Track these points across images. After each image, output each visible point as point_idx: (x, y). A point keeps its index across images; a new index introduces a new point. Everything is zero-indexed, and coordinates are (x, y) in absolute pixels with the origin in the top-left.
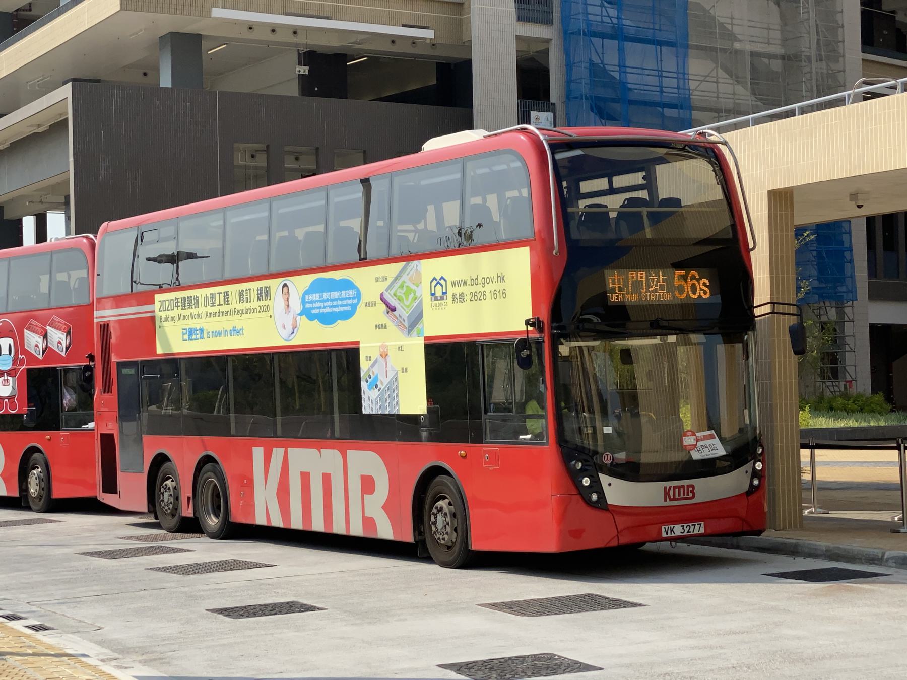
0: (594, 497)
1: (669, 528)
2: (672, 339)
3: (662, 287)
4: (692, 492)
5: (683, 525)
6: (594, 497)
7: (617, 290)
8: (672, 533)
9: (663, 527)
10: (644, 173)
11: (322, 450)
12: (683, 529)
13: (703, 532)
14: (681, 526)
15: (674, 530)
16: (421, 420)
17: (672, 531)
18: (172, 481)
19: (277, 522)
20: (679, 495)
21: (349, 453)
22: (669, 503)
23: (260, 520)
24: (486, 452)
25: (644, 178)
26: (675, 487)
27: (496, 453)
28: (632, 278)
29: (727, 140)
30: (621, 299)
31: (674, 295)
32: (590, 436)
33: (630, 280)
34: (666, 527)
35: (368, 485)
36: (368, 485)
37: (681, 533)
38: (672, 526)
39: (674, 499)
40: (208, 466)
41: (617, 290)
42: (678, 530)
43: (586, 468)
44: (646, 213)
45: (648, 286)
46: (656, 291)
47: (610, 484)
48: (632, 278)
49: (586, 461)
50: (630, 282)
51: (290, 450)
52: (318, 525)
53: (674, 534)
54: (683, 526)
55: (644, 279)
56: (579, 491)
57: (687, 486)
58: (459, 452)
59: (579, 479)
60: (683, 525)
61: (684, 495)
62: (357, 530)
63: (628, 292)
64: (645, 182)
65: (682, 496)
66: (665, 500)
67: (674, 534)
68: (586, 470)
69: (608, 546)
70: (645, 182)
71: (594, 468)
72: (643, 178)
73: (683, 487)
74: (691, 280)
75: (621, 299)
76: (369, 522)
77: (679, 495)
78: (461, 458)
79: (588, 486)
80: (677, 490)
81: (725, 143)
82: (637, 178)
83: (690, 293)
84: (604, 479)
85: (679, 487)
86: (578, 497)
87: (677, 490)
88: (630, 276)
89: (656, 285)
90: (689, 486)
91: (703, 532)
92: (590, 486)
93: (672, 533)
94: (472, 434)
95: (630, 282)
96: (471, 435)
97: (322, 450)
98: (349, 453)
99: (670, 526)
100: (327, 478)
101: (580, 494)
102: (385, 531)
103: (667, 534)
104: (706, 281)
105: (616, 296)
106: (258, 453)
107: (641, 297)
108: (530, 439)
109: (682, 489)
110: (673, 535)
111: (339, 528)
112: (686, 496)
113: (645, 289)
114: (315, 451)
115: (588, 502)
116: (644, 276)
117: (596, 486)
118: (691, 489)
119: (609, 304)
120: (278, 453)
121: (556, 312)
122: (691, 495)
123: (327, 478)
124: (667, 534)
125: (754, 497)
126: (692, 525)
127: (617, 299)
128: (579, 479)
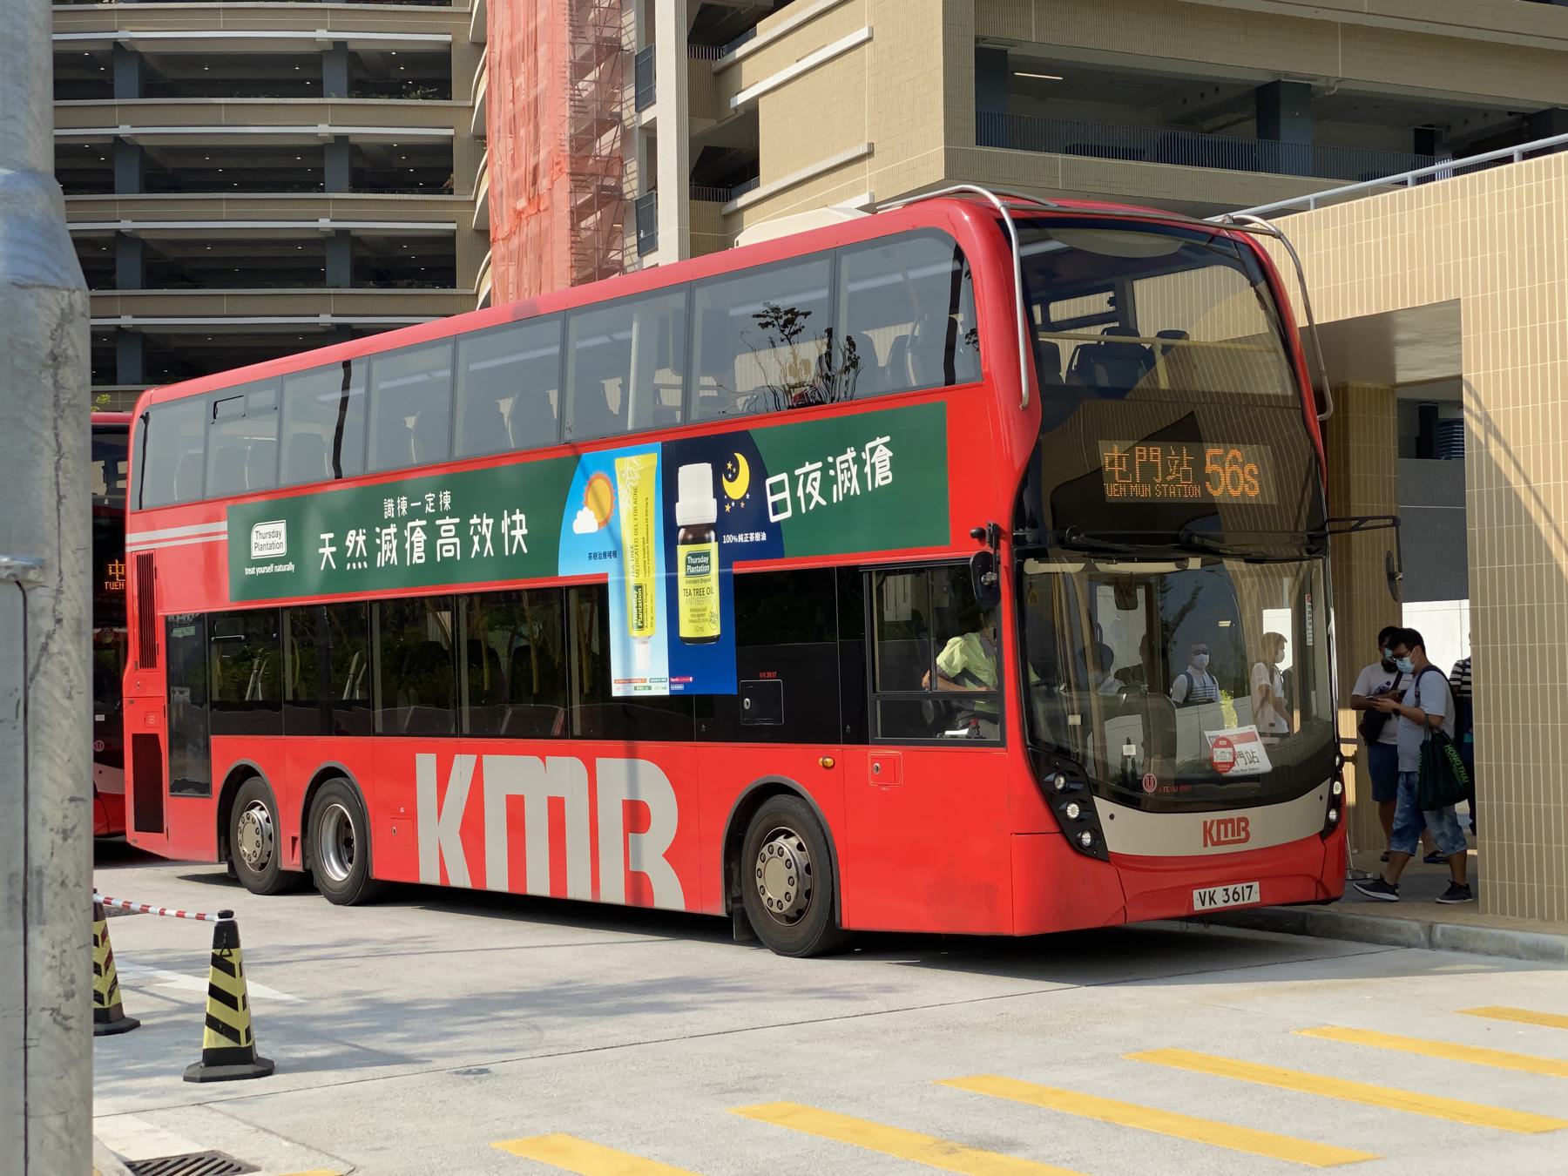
0: (1087, 838)
1: (1246, 897)
2: (1195, 563)
3: (1186, 475)
4: (1245, 829)
5: (1226, 887)
6: (1087, 838)
7: (1117, 478)
8: (1212, 902)
9: (1196, 893)
10: (1111, 294)
11: (547, 758)
12: (1227, 894)
13: (1258, 899)
14: (1224, 890)
15: (1214, 897)
16: (745, 706)
17: (1211, 899)
18: (262, 809)
19: (460, 878)
20: (1226, 836)
21: (600, 762)
22: (1212, 850)
23: (428, 875)
24: (876, 759)
25: (1111, 302)
26: (1220, 822)
27: (894, 760)
28: (1141, 457)
29: (1282, 231)
30: (1123, 492)
31: (1204, 489)
32: (1078, 731)
33: (1138, 460)
34: (1202, 891)
35: (636, 816)
36: (636, 816)
37: (1224, 901)
38: (1212, 890)
39: (1219, 843)
40: (330, 785)
41: (1117, 478)
42: (1220, 898)
43: (1073, 786)
44: (1160, 347)
45: (1166, 473)
46: (1176, 481)
47: (1112, 817)
48: (1141, 457)
49: (1072, 774)
50: (1137, 466)
51: (486, 758)
52: (538, 885)
53: (1215, 903)
54: (1226, 890)
55: (1159, 461)
56: (1061, 828)
57: (1238, 819)
58: (821, 760)
59: (1061, 808)
60: (1226, 887)
61: (1233, 835)
62: (614, 893)
63: (1134, 483)
64: (1112, 308)
65: (1230, 837)
66: (1206, 845)
67: (1215, 903)
68: (1072, 791)
69: (1110, 924)
70: (1112, 308)
71: (1085, 791)
72: (1108, 302)
73: (1231, 821)
74: (1231, 466)
75: (1123, 492)
76: (636, 881)
77: (1226, 836)
78: (823, 769)
79: (1076, 818)
80: (1222, 826)
81: (1278, 235)
82: (1098, 303)
83: (1230, 487)
84: (1103, 807)
85: (1225, 822)
86: (1059, 838)
87: (1222, 826)
88: (1137, 454)
89: (1178, 472)
90: (1240, 820)
91: (1258, 899)
92: (1078, 820)
93: (1212, 902)
94: (848, 727)
95: (1137, 466)
96: (844, 729)
97: (547, 758)
98: (600, 762)
99: (1207, 890)
100: (556, 807)
101: (1062, 832)
102: (669, 895)
103: (1203, 904)
104: (1254, 468)
105: (1117, 487)
106: (426, 764)
107: (1153, 492)
108: (967, 737)
109: (1230, 825)
110: (1213, 906)
111: (578, 889)
112: (1236, 838)
113: (1160, 477)
114: (536, 759)
115: (1077, 847)
116: (1159, 453)
117: (1090, 820)
118: (1243, 824)
119: (1107, 501)
120: (463, 765)
121: (1019, 516)
122: (1243, 835)
123: (556, 807)
124: (1203, 904)
125: (1332, 841)
126: (1247, 887)
127: (1116, 493)
128: (1061, 808)
